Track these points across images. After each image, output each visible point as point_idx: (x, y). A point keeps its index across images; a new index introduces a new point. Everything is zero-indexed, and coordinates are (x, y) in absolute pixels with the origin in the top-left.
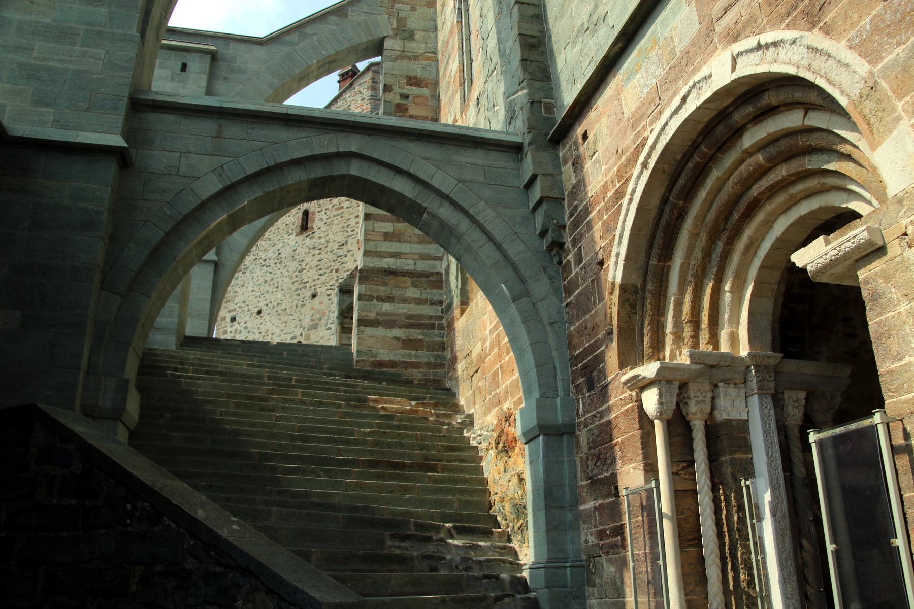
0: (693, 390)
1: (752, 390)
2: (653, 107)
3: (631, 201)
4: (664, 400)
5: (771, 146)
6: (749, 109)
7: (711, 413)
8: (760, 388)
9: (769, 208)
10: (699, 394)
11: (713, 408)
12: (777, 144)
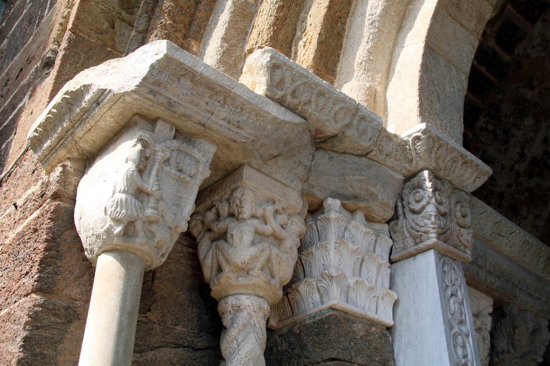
0: (254, 192)
1: (418, 239)
4: (151, 185)
7: (288, 289)
8: (442, 234)
10: (270, 209)
11: (300, 271)
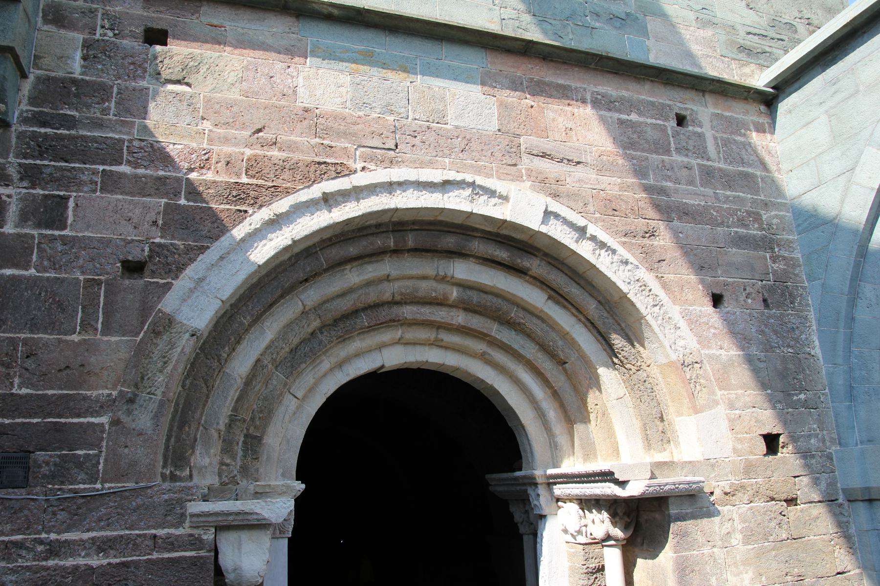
2: (376, 142)
3: (275, 223)
5: (475, 292)
6: (502, 254)
9: (398, 333)
12: (485, 296)
